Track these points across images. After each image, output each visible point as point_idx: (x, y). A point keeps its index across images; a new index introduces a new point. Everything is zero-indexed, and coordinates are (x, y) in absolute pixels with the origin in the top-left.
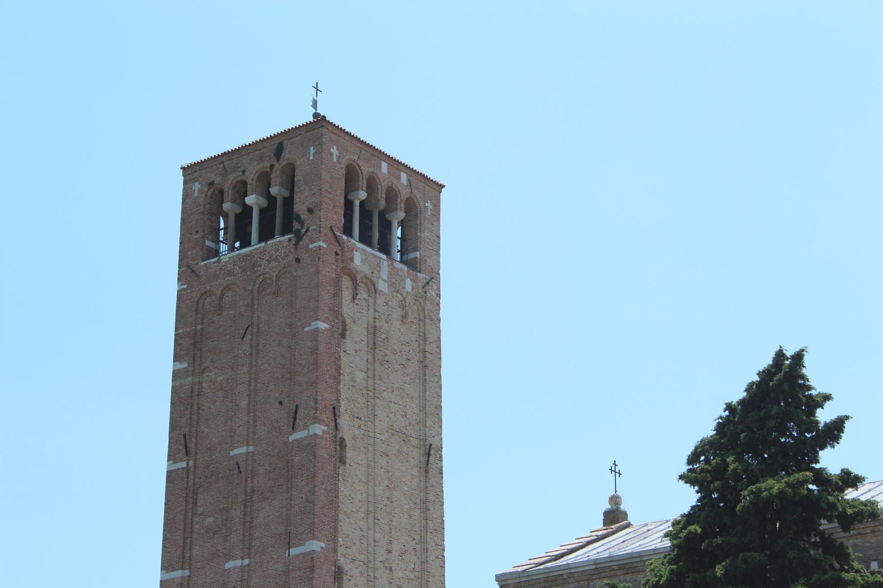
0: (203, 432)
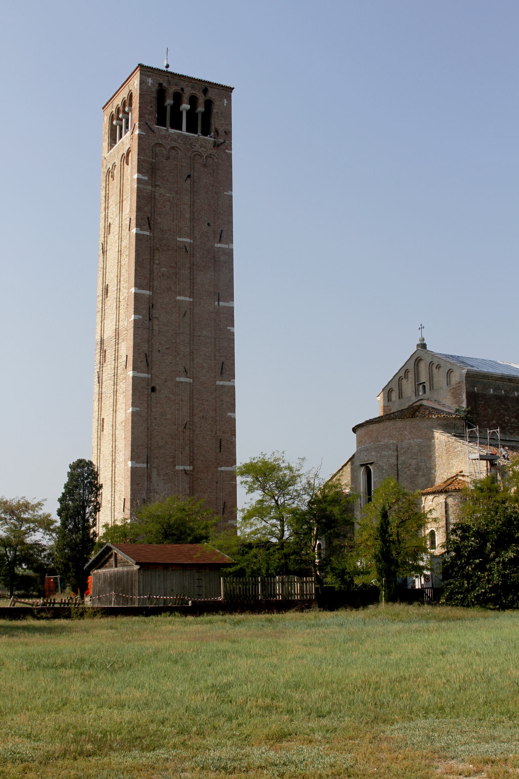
0: (157, 220)
